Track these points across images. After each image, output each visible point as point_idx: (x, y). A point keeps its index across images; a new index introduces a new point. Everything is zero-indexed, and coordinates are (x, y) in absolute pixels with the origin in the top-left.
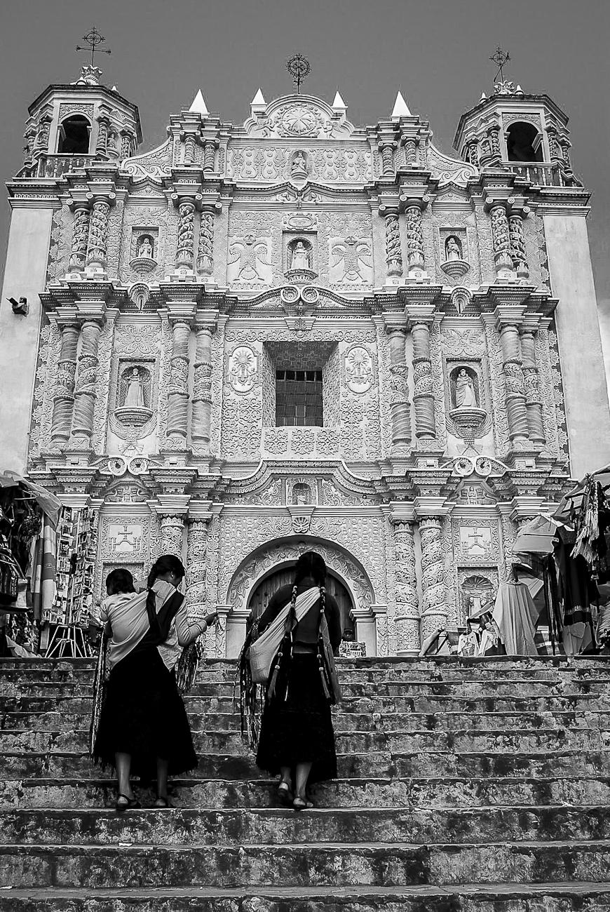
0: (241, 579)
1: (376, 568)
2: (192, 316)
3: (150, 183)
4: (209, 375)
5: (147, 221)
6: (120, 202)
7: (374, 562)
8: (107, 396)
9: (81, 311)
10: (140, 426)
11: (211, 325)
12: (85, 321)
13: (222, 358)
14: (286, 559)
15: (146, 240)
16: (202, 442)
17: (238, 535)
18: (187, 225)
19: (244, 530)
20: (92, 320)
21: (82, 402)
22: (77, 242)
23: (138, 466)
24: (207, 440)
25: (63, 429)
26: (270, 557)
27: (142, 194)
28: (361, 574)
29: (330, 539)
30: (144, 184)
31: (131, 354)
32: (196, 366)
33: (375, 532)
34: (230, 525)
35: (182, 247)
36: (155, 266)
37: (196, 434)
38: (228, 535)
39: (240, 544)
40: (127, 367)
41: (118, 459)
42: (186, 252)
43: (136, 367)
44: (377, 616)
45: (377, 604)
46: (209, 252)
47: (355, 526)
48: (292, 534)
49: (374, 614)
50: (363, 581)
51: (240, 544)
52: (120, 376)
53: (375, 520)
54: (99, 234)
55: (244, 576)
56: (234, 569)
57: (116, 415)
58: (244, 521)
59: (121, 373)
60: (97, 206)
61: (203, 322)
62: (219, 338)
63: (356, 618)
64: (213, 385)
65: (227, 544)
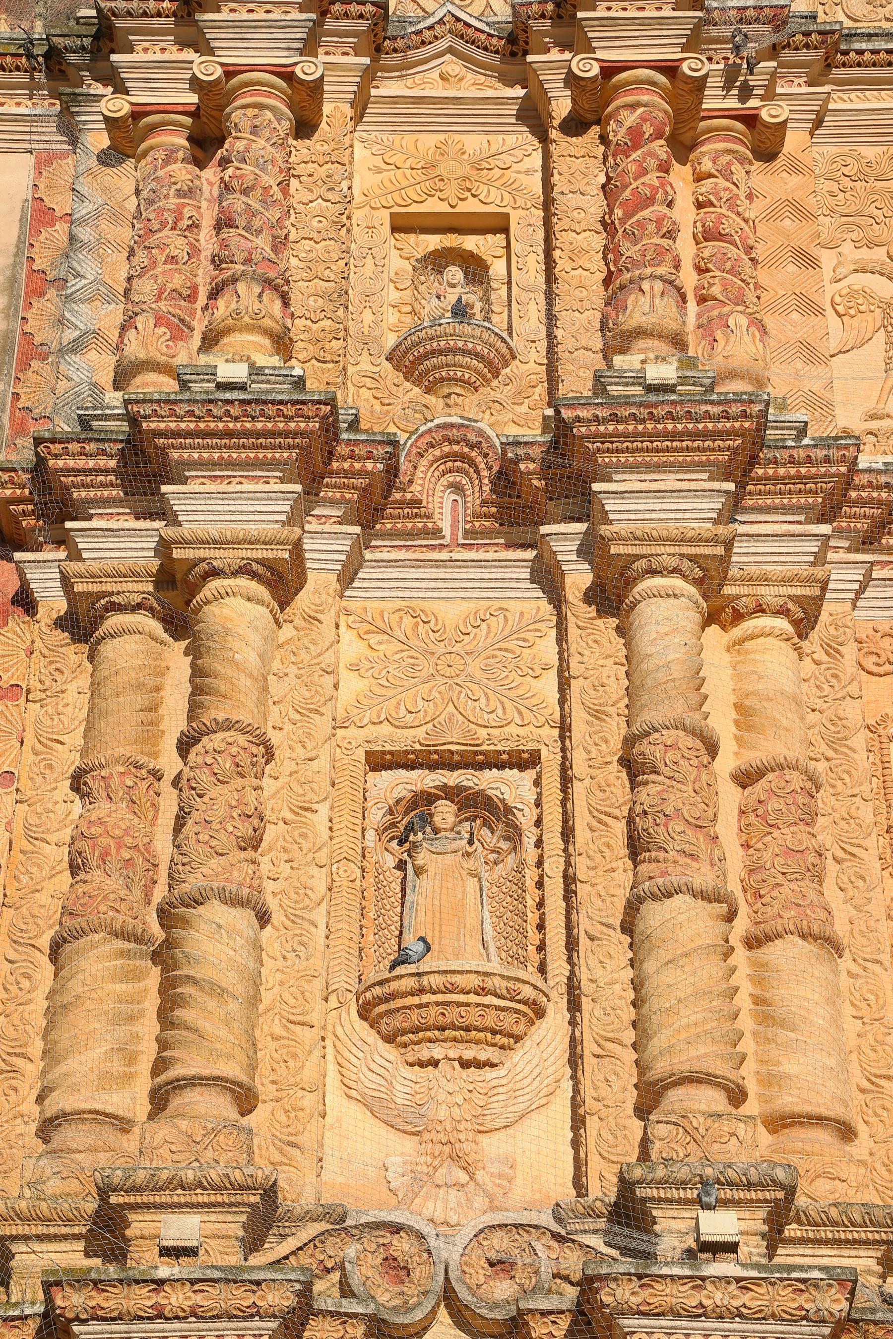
2: (714, 540)
3: (460, 45)
4: (809, 818)
5: (451, 191)
6: (334, 109)
8: (320, 915)
9: (186, 530)
10: (489, 1064)
11: (799, 591)
12: (215, 573)
13: (860, 740)
15: (455, 273)
16: (822, 1136)
18: (652, 178)
20: (244, 570)
21: (216, 941)
22: (154, 263)
23: (499, 1266)
24: (846, 1132)
25: (106, 1081)
27: (426, 82)
30: (429, 50)
31: (420, 733)
32: (745, 778)
35: (636, 264)
36: (506, 364)
37: (789, 1101)
40: (401, 792)
41: (397, 1229)
42: (659, 286)
43: (449, 793)
46: (751, 297)
52: (371, 835)
54: (257, 223)
57: (364, 1013)
59: (377, 816)
60: (238, 116)
61: (765, 579)
62: (833, 650)
64: (832, 868)
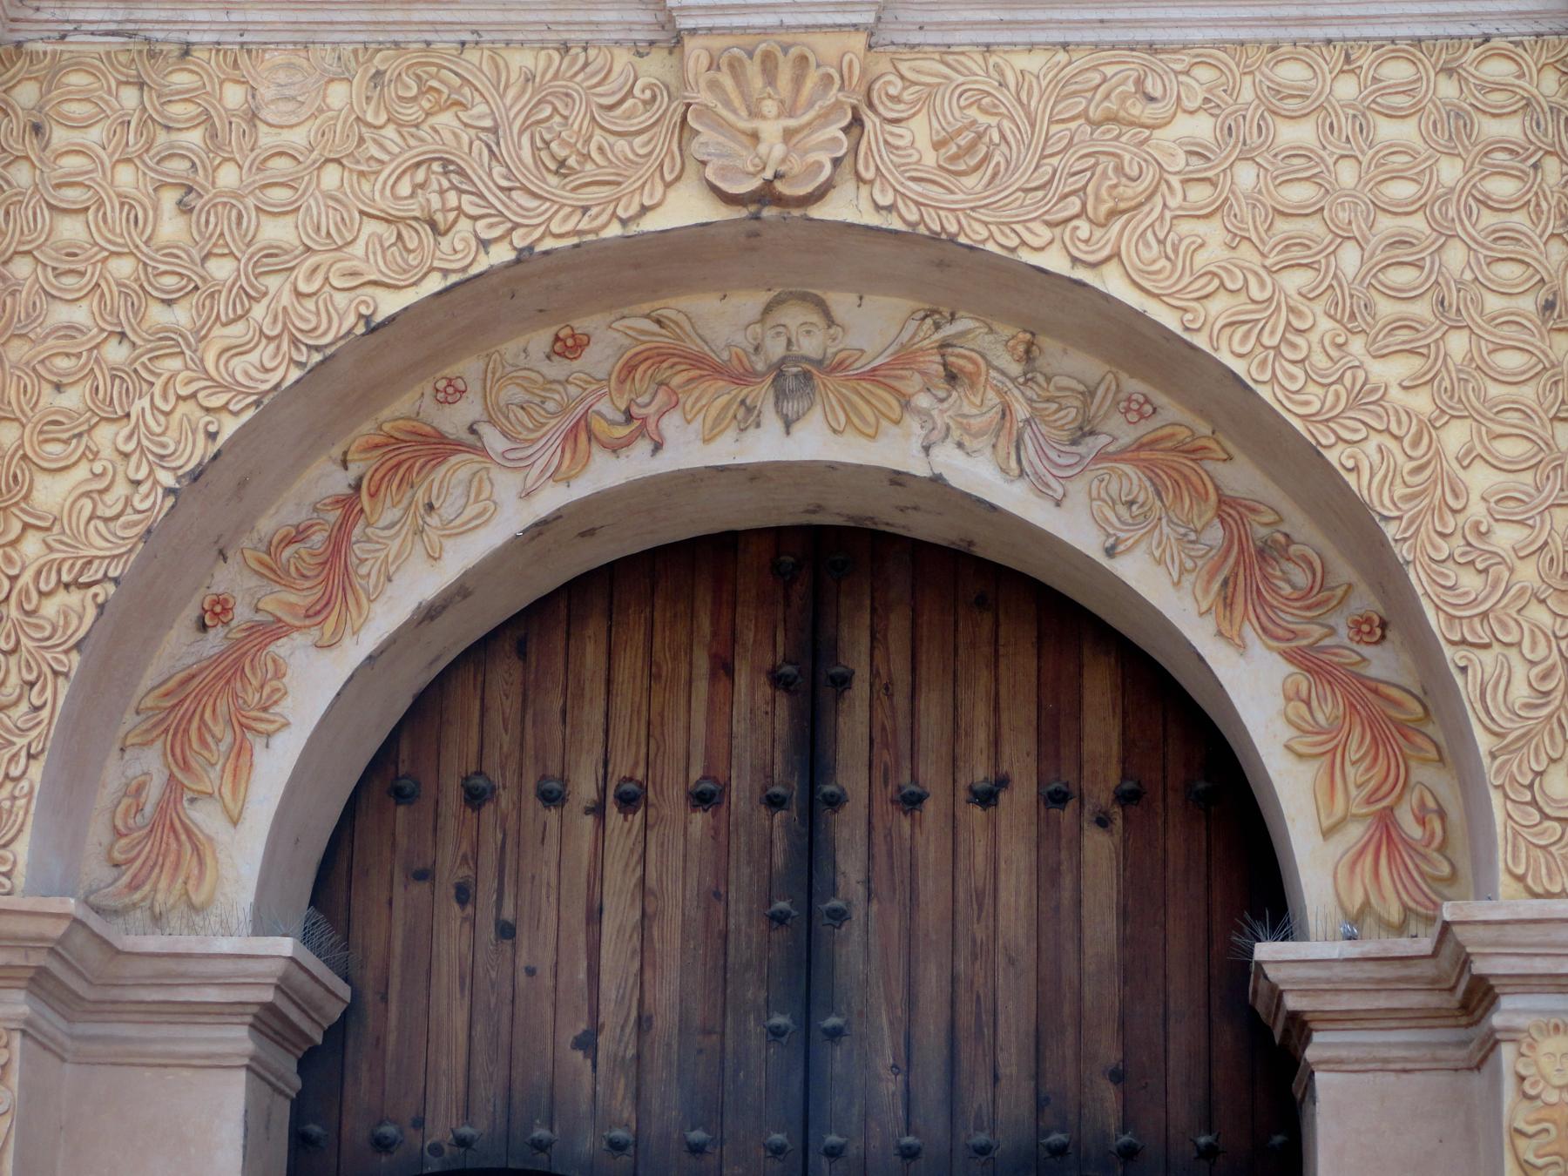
0: (215, 641)
1: (1506, 537)
7: (1480, 479)
14: (637, 465)
17: (171, 227)
19: (228, 177)
26: (493, 440)
28: (1365, 602)
29: (1054, 261)
33: (1502, 188)
34: (95, 135)
38: (71, 229)
39: (181, 316)
44: (1509, 1012)
45: (1509, 902)
47: (1302, 133)
48: (685, 208)
49: (1478, 997)
50: (1383, 663)
51: (181, 316)
53: (1498, 69)
55: (242, 614)
56: (108, 547)
58: (234, 96)
63: (1300, 1026)
65: (61, 314)
